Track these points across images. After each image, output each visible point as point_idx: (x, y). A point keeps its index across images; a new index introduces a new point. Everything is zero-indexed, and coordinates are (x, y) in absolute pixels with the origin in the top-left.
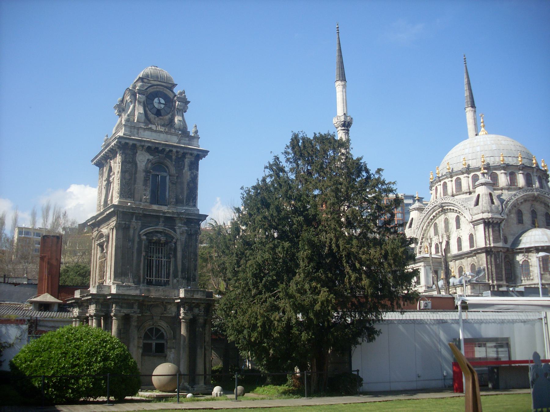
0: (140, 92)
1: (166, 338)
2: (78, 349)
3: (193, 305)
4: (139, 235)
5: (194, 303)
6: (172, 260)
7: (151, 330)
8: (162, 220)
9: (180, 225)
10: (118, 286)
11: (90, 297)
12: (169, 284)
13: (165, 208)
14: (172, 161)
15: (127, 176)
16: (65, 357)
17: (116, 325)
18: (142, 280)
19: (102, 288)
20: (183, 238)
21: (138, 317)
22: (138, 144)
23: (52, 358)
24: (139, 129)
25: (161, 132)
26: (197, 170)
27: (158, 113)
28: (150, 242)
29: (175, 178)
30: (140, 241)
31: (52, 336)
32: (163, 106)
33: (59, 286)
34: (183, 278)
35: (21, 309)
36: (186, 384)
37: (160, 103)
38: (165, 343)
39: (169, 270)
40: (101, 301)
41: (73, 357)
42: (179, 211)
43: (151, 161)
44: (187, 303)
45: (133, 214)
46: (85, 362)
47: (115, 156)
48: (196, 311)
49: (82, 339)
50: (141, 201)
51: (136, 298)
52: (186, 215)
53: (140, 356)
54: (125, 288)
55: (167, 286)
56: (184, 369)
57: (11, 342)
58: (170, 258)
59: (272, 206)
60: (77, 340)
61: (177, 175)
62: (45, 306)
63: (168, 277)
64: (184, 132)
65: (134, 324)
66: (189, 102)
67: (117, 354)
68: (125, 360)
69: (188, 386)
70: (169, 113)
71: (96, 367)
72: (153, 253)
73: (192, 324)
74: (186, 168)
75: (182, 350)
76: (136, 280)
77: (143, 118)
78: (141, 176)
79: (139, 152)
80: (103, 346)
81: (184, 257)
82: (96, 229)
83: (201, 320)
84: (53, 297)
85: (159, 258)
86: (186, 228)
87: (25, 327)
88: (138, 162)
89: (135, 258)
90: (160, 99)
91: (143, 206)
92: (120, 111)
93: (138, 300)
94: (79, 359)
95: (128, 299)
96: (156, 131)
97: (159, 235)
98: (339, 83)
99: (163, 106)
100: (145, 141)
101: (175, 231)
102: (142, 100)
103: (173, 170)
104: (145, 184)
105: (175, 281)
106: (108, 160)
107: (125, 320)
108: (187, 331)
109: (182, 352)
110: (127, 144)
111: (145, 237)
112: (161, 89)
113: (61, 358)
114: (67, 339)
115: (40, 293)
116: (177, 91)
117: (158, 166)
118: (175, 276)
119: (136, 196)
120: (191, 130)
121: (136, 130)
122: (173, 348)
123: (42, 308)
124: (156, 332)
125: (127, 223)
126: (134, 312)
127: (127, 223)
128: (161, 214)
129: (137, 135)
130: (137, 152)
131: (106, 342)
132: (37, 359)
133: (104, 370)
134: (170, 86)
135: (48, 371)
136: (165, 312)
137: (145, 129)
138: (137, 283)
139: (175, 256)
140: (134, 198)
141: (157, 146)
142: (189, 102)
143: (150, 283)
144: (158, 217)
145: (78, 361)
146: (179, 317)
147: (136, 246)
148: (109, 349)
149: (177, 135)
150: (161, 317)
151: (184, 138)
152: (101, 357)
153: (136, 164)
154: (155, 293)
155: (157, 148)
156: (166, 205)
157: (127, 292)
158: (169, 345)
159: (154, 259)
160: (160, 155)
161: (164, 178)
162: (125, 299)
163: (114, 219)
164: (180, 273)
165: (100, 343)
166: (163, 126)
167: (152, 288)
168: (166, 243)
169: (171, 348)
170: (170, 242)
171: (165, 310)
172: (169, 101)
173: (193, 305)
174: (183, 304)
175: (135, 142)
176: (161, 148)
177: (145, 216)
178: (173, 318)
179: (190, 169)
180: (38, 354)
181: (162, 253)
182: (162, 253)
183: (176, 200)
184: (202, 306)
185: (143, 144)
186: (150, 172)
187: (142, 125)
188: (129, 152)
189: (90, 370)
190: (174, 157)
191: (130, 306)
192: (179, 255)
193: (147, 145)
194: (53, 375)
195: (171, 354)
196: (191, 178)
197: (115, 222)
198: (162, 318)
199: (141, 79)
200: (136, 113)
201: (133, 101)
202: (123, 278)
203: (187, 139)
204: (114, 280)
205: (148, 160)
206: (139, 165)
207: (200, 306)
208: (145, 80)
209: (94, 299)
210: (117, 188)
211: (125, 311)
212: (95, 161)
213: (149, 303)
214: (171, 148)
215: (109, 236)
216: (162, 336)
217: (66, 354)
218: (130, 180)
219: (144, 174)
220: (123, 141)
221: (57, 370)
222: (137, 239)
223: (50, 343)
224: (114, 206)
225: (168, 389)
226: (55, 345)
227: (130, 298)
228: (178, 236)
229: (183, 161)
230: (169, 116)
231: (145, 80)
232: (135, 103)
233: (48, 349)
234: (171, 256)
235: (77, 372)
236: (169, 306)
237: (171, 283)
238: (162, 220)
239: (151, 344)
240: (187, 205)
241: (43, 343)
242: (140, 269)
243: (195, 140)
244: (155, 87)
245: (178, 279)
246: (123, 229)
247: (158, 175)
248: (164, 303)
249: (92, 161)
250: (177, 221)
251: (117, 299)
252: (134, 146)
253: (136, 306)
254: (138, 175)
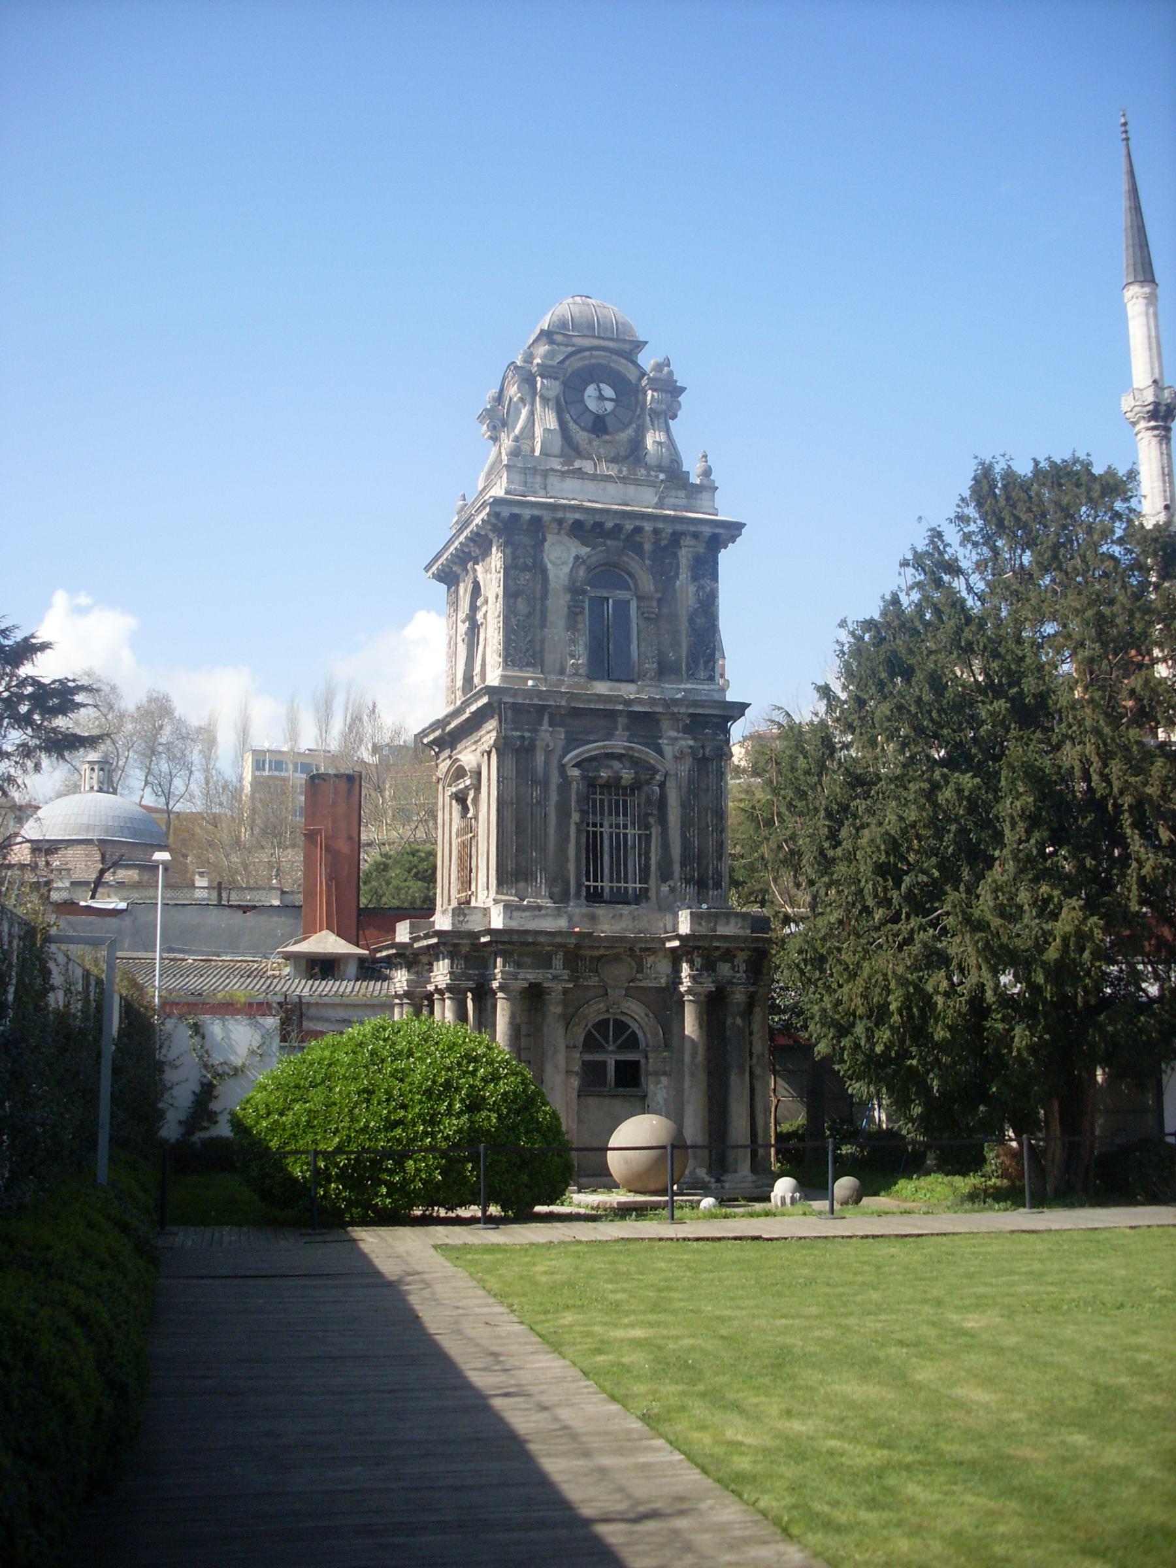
0: (545, 371)
1: (642, 1044)
2: (402, 1080)
3: (717, 954)
4: (562, 768)
5: (717, 948)
6: (655, 831)
7: (602, 1025)
8: (622, 721)
9: (673, 734)
10: (508, 907)
11: (435, 940)
12: (648, 899)
13: (628, 690)
14: (642, 558)
15: (521, 606)
16: (368, 1101)
17: (507, 1013)
18: (572, 891)
19: (465, 915)
20: (684, 769)
21: (566, 991)
22: (546, 516)
23: (335, 1104)
24: (546, 473)
25: (609, 478)
26: (715, 578)
27: (599, 426)
28: (591, 784)
29: (655, 604)
30: (566, 782)
31: (335, 1048)
32: (609, 406)
33: (359, 909)
34: (688, 881)
35: (261, 974)
36: (702, 1173)
37: (601, 398)
38: (643, 1061)
39: (648, 859)
40: (464, 950)
41: (388, 1100)
42: (668, 695)
43: (584, 562)
44: (698, 948)
45: (541, 709)
46: (420, 1115)
47: (486, 553)
48: (724, 969)
49: (410, 1054)
50: (562, 672)
51: (558, 940)
52: (687, 707)
53: (574, 1095)
54: (527, 914)
55: (644, 905)
56: (693, 1132)
57: (238, 1062)
58: (648, 827)
59: (919, 675)
60: (398, 1056)
61: (659, 595)
62: (323, 967)
63: (645, 878)
64: (674, 476)
65: (555, 1009)
66: (683, 389)
67: (506, 1093)
68: (526, 1109)
69: (707, 1179)
70: (629, 424)
71: (450, 1126)
72: (602, 814)
73: (714, 1005)
74: (684, 575)
75: (687, 1078)
76: (556, 890)
77: (557, 444)
78: (558, 603)
79: (550, 538)
80: (467, 1072)
81: (686, 824)
82: (447, 753)
83: (739, 996)
84: (343, 942)
85: (618, 826)
86: (691, 743)
87: (271, 1022)
88: (549, 566)
89: (552, 830)
90: (602, 385)
91: (569, 687)
92: (494, 428)
93: (561, 945)
94: (404, 1107)
95: (534, 944)
96: (594, 478)
97: (617, 765)
98: (1135, 289)
99: (609, 406)
100: (564, 507)
101: (659, 751)
102: (552, 394)
103: (647, 583)
104: (572, 625)
105: (665, 889)
106: (470, 565)
107: (532, 999)
108: (701, 1027)
109: (687, 1085)
110: (515, 517)
111: (576, 772)
112: (601, 358)
113: (356, 1103)
114: (373, 1053)
115: (309, 930)
116: (647, 360)
117: (607, 574)
118: (665, 876)
119: (549, 659)
120: (693, 468)
121: (539, 479)
122: (665, 1074)
123: (317, 970)
124: (617, 1031)
125: (527, 734)
126: (555, 978)
127: (527, 734)
128: (620, 707)
129: (542, 493)
130: (544, 540)
131: (475, 1059)
132: (297, 1107)
133: (473, 1135)
134: (627, 347)
135: (324, 1138)
136: (639, 976)
137: (563, 474)
138: (562, 898)
139: (663, 821)
140: (542, 665)
141: (598, 518)
142: (683, 389)
143: (595, 897)
144: (611, 715)
145: (402, 1113)
146: (676, 989)
147: (554, 797)
148: (483, 1079)
149: (652, 484)
150: (627, 989)
151: (673, 493)
152: (462, 1101)
153: (544, 572)
154: (611, 923)
155: (598, 525)
156: (632, 681)
157: (532, 925)
158: (653, 1063)
159: (606, 830)
160: (609, 542)
161: (622, 607)
162: (528, 944)
163: (492, 724)
164: (677, 868)
165: (459, 1064)
166: (614, 460)
167: (601, 911)
168: (636, 786)
169: (657, 1074)
170: (648, 782)
171: (640, 969)
172: (628, 391)
173: (717, 954)
174: (688, 953)
175: (536, 512)
176: (609, 525)
177: (576, 713)
178: (660, 990)
179: (695, 578)
180: (298, 1093)
181: (625, 815)
182: (625, 815)
183: (659, 663)
184: (741, 957)
185: (560, 515)
186: (584, 592)
187: (556, 464)
188: (526, 540)
189: (433, 1135)
190: (647, 547)
191: (544, 961)
192: (674, 816)
193: (572, 516)
194: (339, 1150)
195: (658, 1090)
196: (699, 601)
197: (494, 734)
198: (629, 993)
199: (547, 335)
200: (538, 432)
201: (528, 399)
202: (521, 885)
203: (682, 494)
204: (497, 893)
205: (577, 558)
206: (551, 576)
207: (735, 956)
208: (559, 338)
209: (444, 944)
210: (496, 641)
211: (531, 975)
212: (434, 568)
213: (596, 953)
214: (638, 523)
215: (479, 774)
216: (632, 1042)
217: (370, 1092)
218: (529, 615)
219: (568, 597)
220: (506, 512)
221: (349, 1136)
222: (555, 779)
223: (330, 1065)
224: (490, 690)
225: (652, 1187)
226: (342, 1071)
227: (541, 939)
228: (669, 765)
229: (675, 556)
230: (630, 431)
231: (559, 338)
232: (533, 403)
233: (323, 1082)
234: (651, 820)
235: (399, 1141)
236: (650, 960)
237: (652, 894)
238: (622, 721)
239: (604, 1064)
240: (692, 677)
241: (311, 1064)
242: (567, 861)
243: (706, 495)
244: (587, 354)
245: (671, 883)
246: (514, 752)
247: (607, 599)
248: (636, 951)
249: (427, 568)
250: (665, 724)
251: (507, 943)
252: (536, 521)
253: (558, 962)
254: (549, 602)
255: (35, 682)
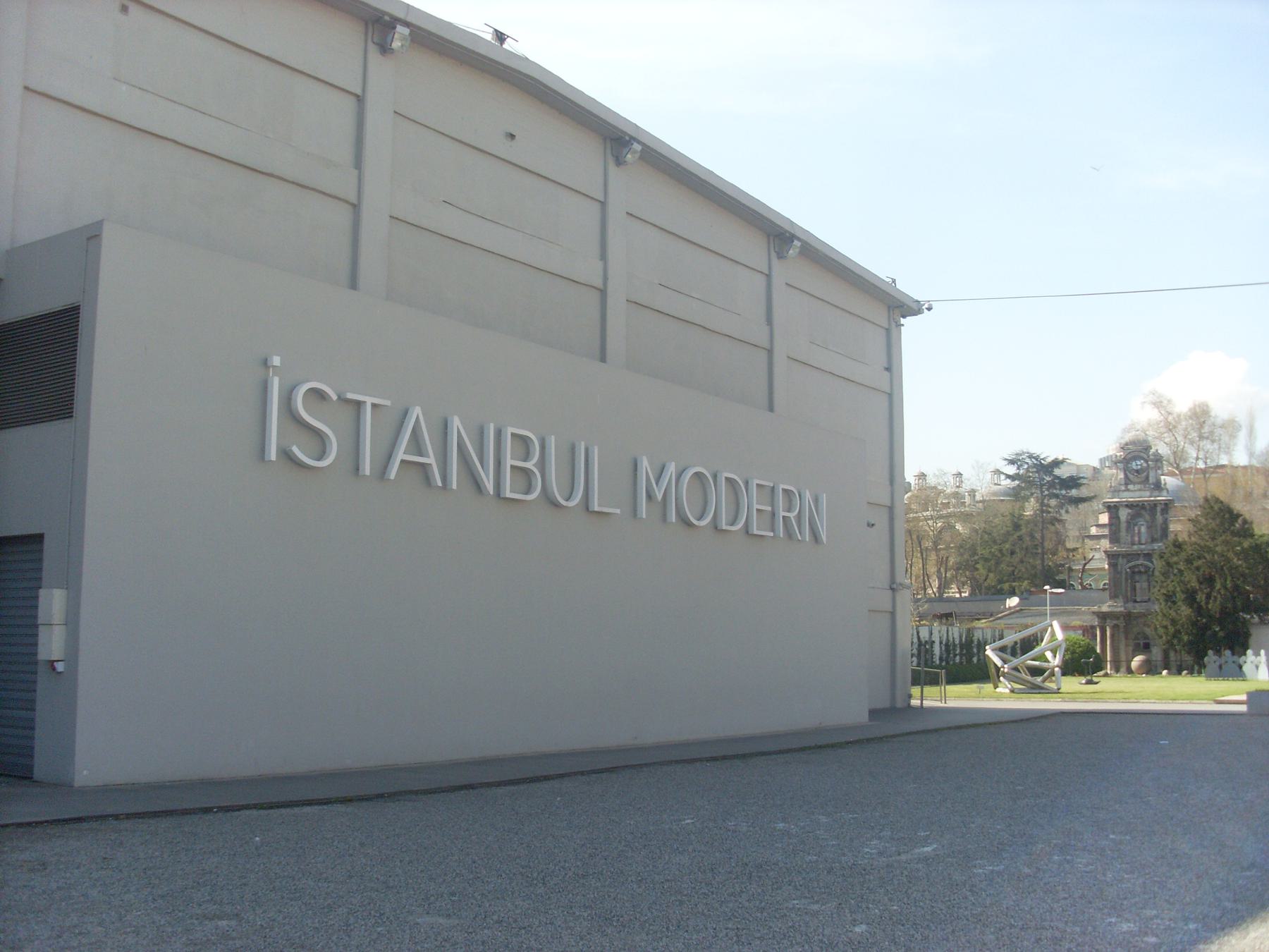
103: (1148, 517)
116: (1152, 451)
191: (1118, 618)
255: (1058, 478)
